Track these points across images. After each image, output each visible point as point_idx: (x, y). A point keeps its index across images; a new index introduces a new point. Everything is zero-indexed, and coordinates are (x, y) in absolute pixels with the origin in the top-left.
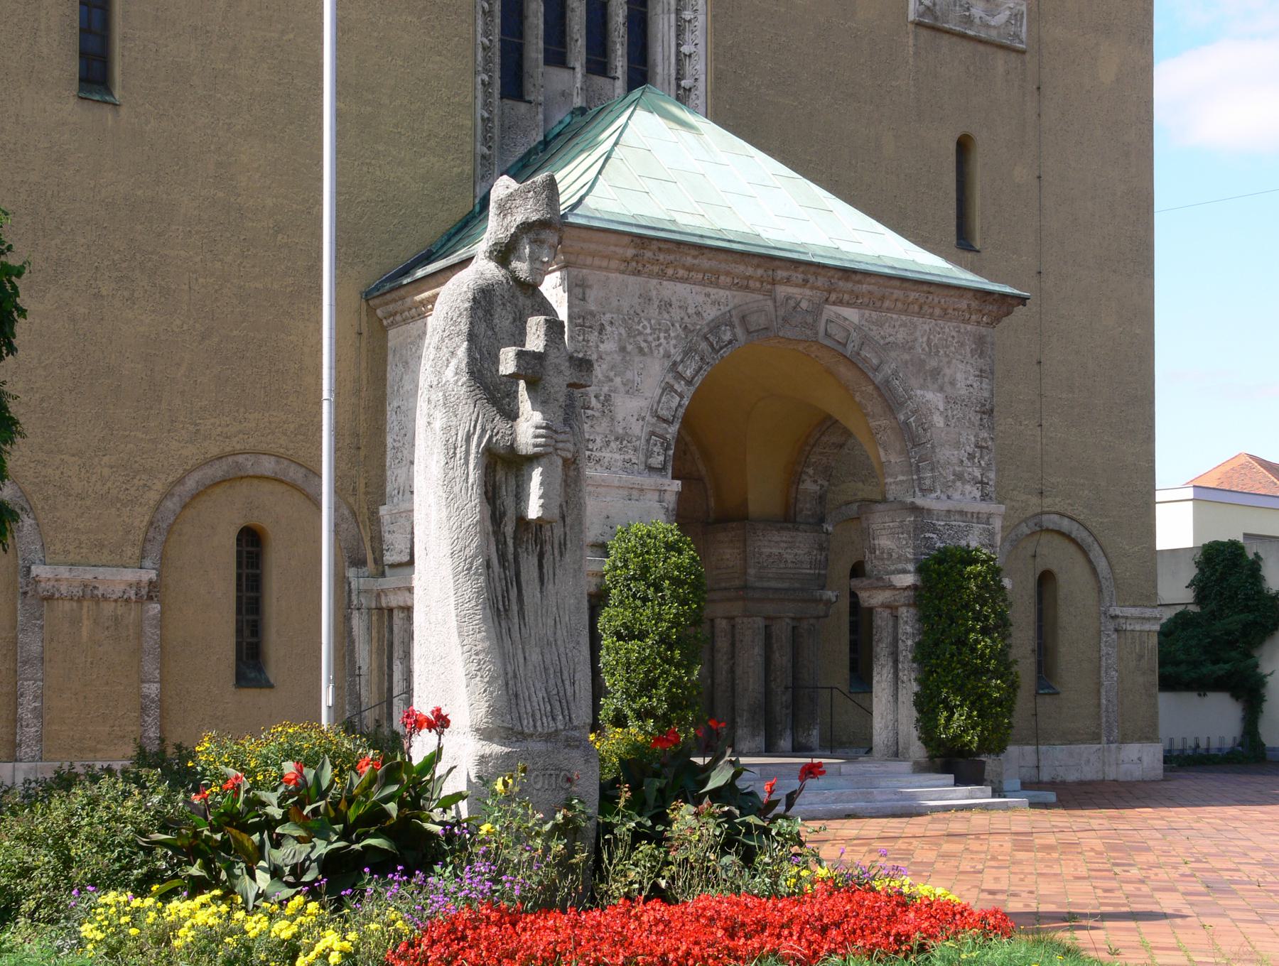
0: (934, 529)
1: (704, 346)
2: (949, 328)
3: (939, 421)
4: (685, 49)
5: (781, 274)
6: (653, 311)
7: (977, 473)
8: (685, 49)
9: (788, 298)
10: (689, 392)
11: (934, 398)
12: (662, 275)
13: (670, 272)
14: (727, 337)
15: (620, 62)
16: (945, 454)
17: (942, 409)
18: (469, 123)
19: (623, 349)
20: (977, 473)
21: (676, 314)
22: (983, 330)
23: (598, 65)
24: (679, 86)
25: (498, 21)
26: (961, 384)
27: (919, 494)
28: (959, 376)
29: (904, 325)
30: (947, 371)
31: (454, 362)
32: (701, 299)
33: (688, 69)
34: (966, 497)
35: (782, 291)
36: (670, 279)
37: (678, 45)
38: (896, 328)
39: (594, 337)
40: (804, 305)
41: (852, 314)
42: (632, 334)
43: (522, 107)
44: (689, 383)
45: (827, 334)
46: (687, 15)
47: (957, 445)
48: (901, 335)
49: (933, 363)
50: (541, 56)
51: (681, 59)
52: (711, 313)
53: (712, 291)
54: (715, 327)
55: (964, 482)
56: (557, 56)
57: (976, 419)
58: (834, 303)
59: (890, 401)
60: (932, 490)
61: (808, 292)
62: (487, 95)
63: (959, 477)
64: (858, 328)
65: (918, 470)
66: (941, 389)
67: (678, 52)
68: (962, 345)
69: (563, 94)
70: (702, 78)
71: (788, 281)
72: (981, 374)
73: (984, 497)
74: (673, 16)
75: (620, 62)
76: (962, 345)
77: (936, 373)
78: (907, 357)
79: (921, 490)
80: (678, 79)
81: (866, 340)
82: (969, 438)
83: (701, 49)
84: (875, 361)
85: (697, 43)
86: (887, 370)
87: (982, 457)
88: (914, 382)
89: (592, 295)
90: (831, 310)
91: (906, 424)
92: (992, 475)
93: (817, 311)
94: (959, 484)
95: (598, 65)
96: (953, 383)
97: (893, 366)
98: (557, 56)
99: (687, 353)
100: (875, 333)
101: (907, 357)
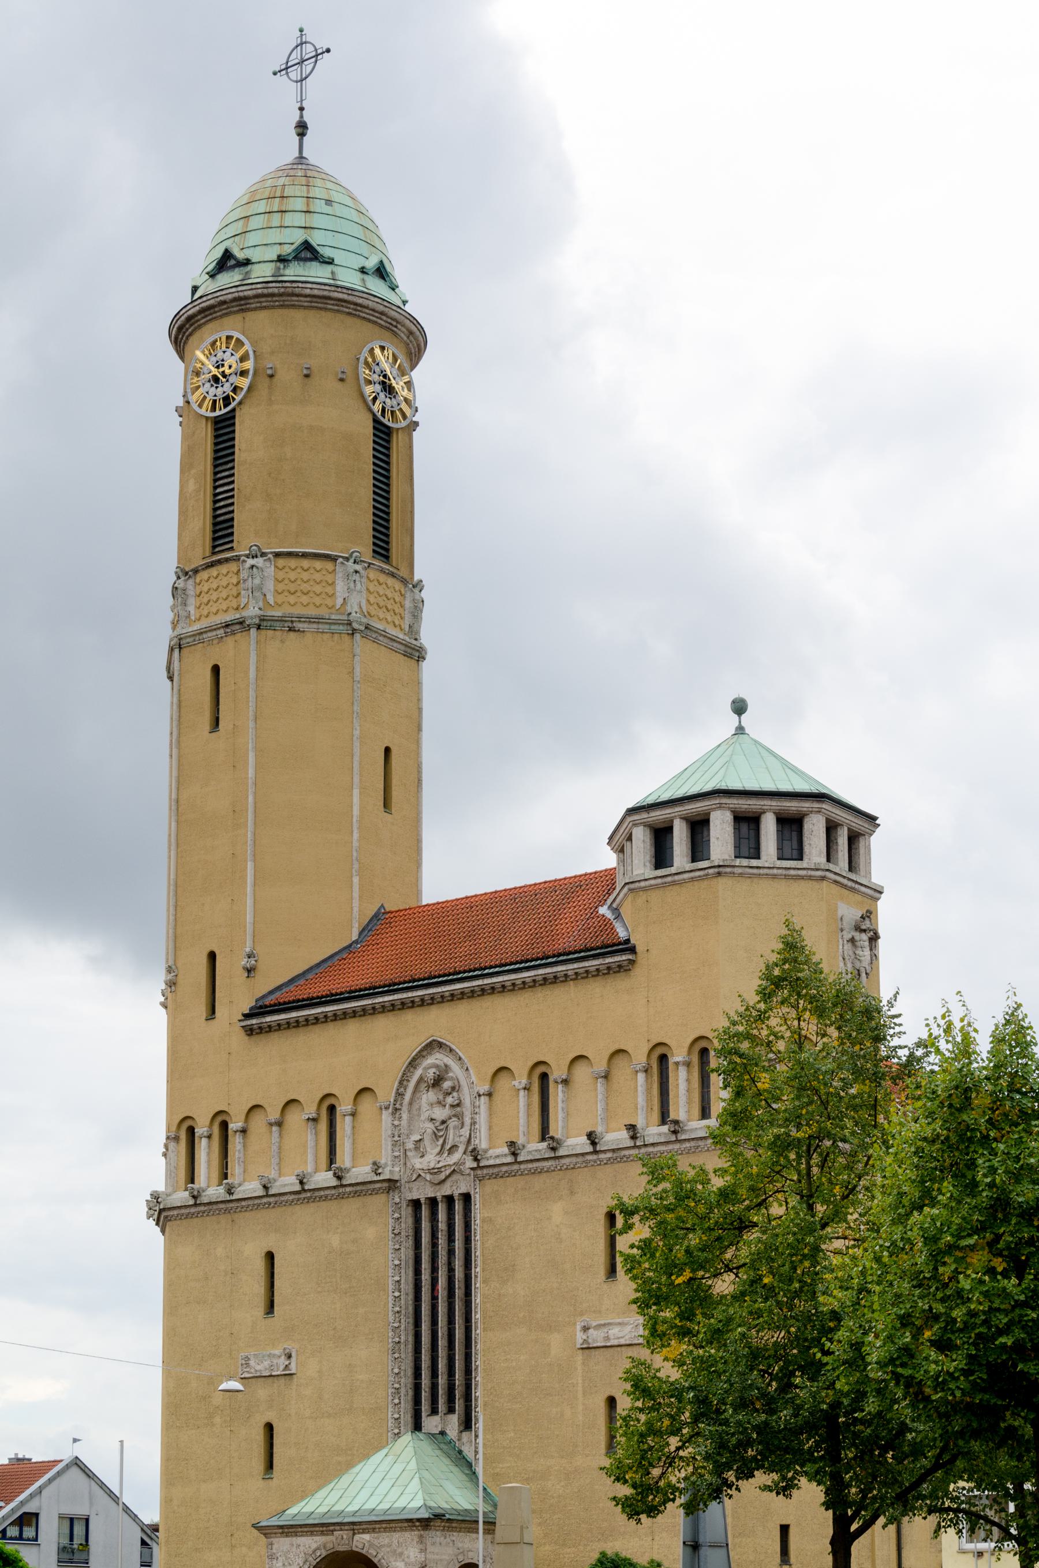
1: (311, 1559)
2: (407, 1534)
5: (332, 1528)
6: (294, 1549)
14: (318, 1554)
19: (284, 1565)
21: (302, 1548)
28: (411, 1554)
29: (388, 1537)
30: (405, 1552)
38: (384, 1539)
39: (274, 1562)
41: (366, 1537)
48: (387, 1541)
49: (400, 1550)
52: (314, 1546)
54: (314, 1551)
66: (403, 1560)
68: (413, 1540)
76: (413, 1540)
77: (401, 1554)
78: (388, 1549)
81: (371, 1545)
86: (379, 1556)
88: (392, 1559)
89: (274, 1547)
90: (357, 1537)
96: (408, 1557)
99: (304, 1563)
100: (376, 1542)
101: (388, 1549)
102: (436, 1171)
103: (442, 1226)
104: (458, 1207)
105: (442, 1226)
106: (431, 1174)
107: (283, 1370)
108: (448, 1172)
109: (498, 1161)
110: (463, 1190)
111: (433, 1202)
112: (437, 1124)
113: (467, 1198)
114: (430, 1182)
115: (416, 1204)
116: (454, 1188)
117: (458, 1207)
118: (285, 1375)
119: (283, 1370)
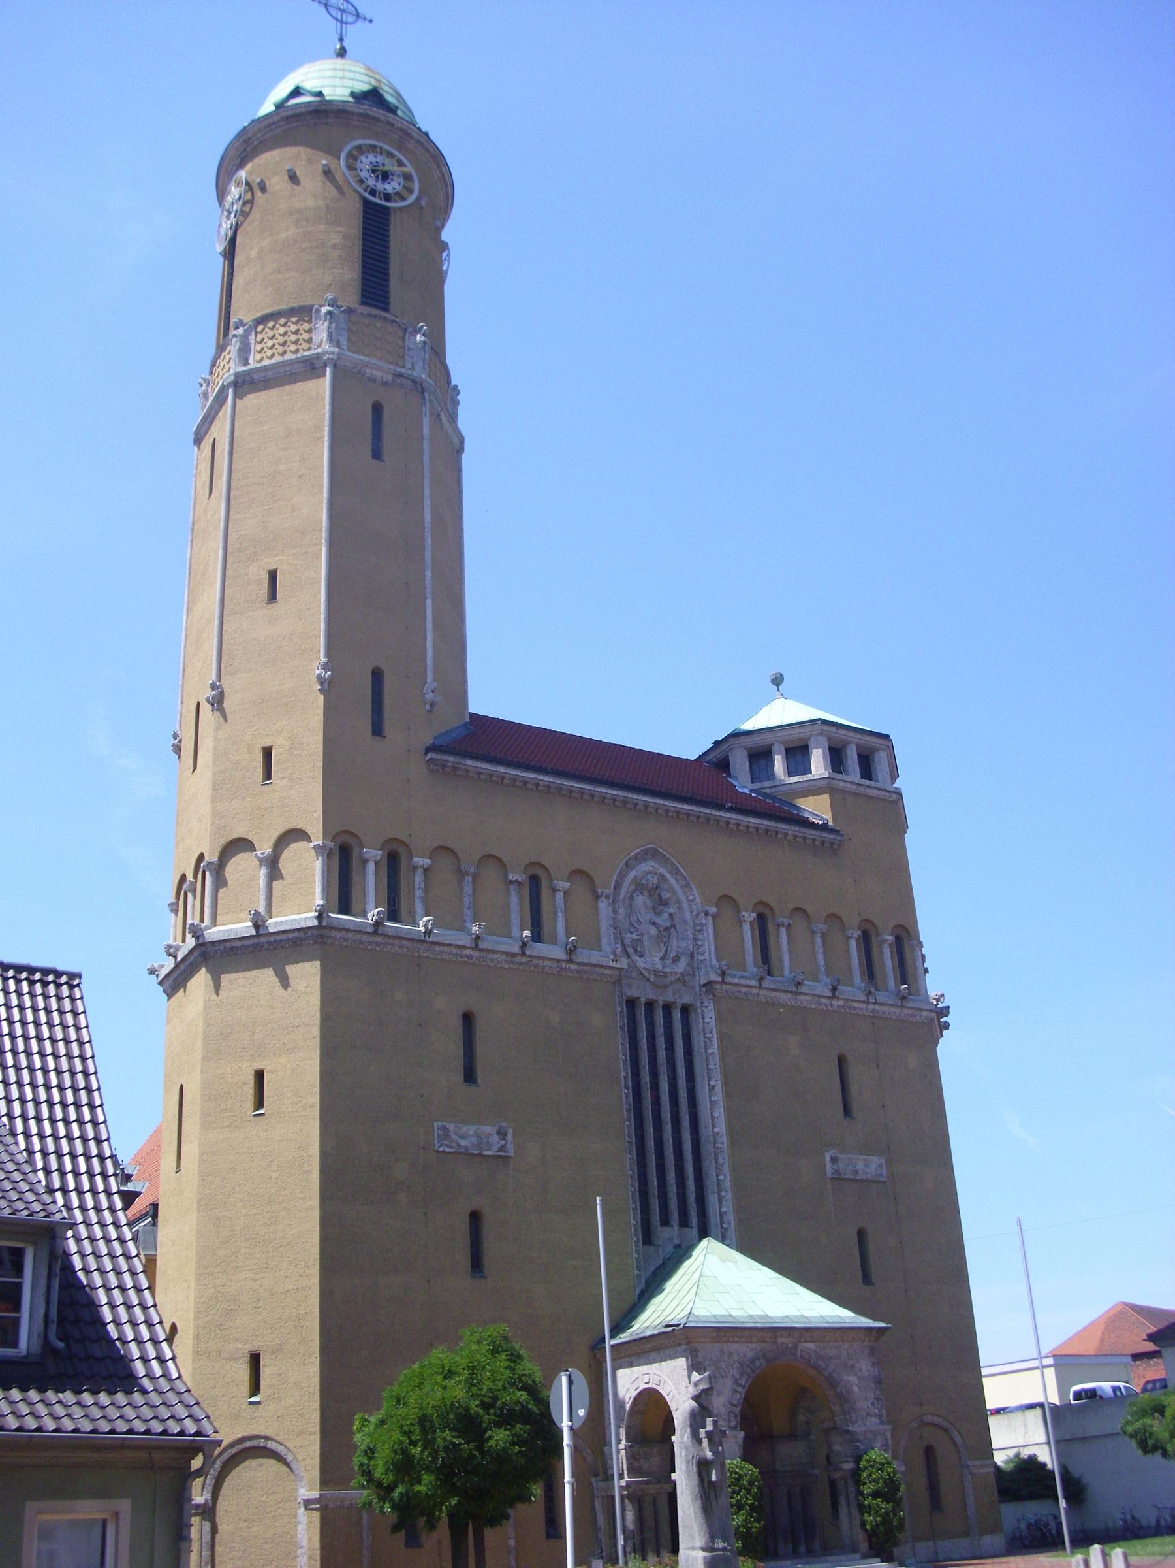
0: (859, 1441)
3: (856, 1389)
4: (724, 1210)
7: (877, 1411)
8: (724, 1210)
9: (783, 1343)
10: (744, 1391)
11: (853, 1379)
12: (728, 1341)
13: (731, 1339)
15: (694, 1220)
16: (861, 1404)
17: (857, 1382)
18: (630, 1262)
20: (877, 1411)
22: (872, 1344)
23: (684, 1223)
24: (722, 1227)
25: (639, 1211)
26: (864, 1369)
27: (850, 1424)
29: (835, 1347)
31: (686, 1435)
32: (745, 1349)
33: (725, 1219)
34: (873, 1423)
35: (780, 1340)
36: (731, 1342)
37: (720, 1208)
40: (790, 1345)
41: (811, 1346)
42: (718, 1368)
43: (652, 1248)
44: (743, 1387)
45: (801, 1356)
46: (723, 1193)
47: (866, 1399)
49: (850, 1362)
50: (659, 1223)
51: (722, 1214)
53: (750, 1345)
55: (871, 1416)
56: (665, 1222)
57: (873, 1385)
58: (804, 1342)
59: (833, 1383)
60: (856, 1422)
61: (791, 1339)
62: (637, 1246)
63: (868, 1414)
64: (815, 1351)
65: (849, 1413)
66: (856, 1375)
67: (720, 1212)
69: (669, 1239)
70: (733, 1223)
71: (782, 1336)
72: (874, 1364)
73: (882, 1422)
74: (716, 1195)
75: (694, 1220)
77: (852, 1367)
78: (838, 1361)
79: (851, 1423)
80: (722, 1224)
82: (871, 1396)
83: (731, 1209)
84: (824, 1366)
85: (728, 1207)
87: (878, 1403)
91: (841, 1392)
92: (884, 1411)
93: (795, 1347)
94: (869, 1418)
95: (684, 1223)
96: (861, 1371)
97: (833, 1367)
98: (665, 1222)
102: (662, 974)
103: (660, 1030)
104: (677, 1015)
105: (660, 1030)
106: (655, 975)
107: (498, 1151)
108: (673, 979)
109: (743, 982)
110: (686, 1000)
111: (650, 1005)
112: (661, 929)
113: (686, 1010)
114: (653, 983)
115: (631, 1003)
116: (677, 996)
117: (677, 1015)
118: (499, 1156)
119: (498, 1151)
